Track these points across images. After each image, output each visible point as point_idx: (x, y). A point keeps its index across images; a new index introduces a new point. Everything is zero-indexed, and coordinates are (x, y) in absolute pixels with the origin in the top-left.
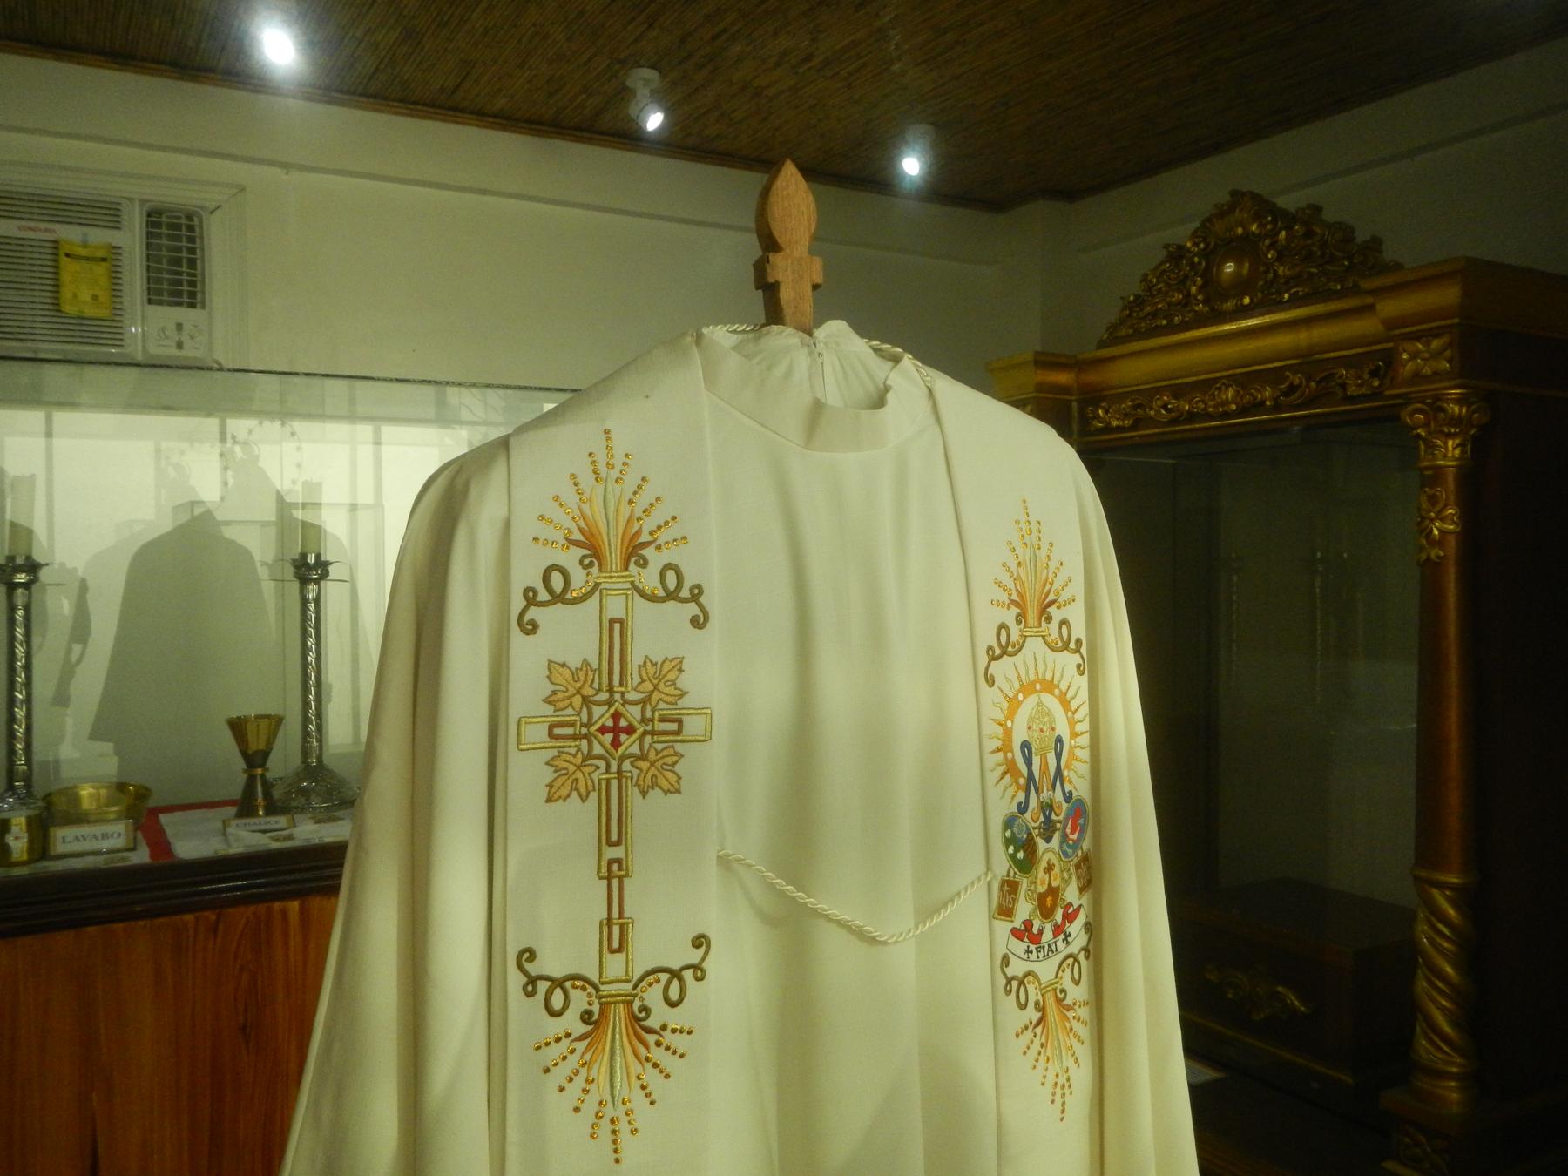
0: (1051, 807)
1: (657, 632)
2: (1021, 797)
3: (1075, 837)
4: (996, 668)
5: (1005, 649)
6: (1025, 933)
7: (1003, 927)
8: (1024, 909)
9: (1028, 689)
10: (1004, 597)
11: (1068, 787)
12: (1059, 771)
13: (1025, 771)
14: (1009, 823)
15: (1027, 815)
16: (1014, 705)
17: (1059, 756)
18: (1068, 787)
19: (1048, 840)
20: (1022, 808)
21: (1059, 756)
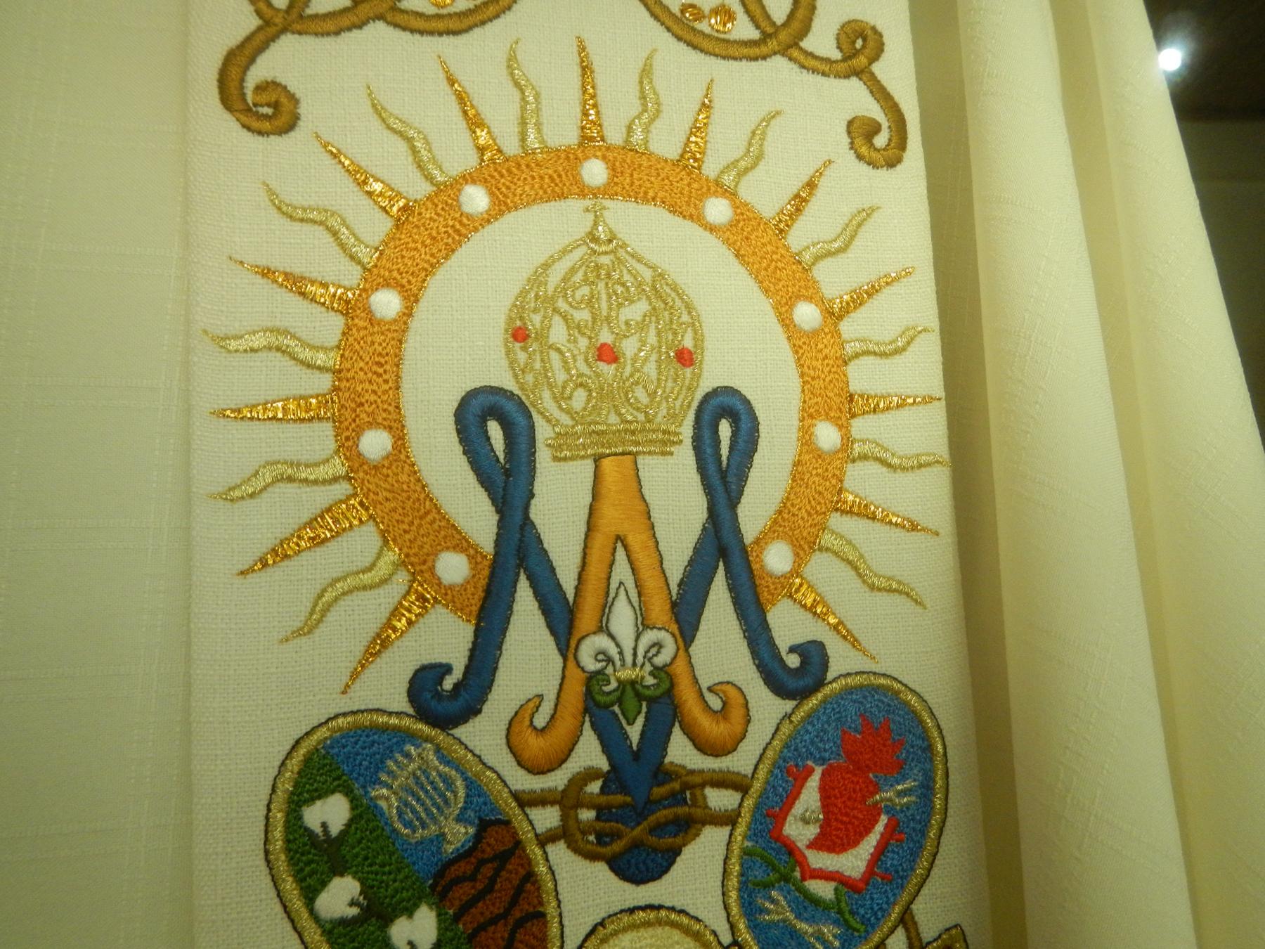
0: (663, 703)
2: (447, 639)
3: (853, 862)
9: (522, 177)
11: (788, 626)
12: (721, 545)
13: (477, 517)
15: (483, 735)
16: (424, 235)
17: (723, 482)
18: (788, 626)
19: (642, 862)
20: (444, 700)
21: (723, 482)
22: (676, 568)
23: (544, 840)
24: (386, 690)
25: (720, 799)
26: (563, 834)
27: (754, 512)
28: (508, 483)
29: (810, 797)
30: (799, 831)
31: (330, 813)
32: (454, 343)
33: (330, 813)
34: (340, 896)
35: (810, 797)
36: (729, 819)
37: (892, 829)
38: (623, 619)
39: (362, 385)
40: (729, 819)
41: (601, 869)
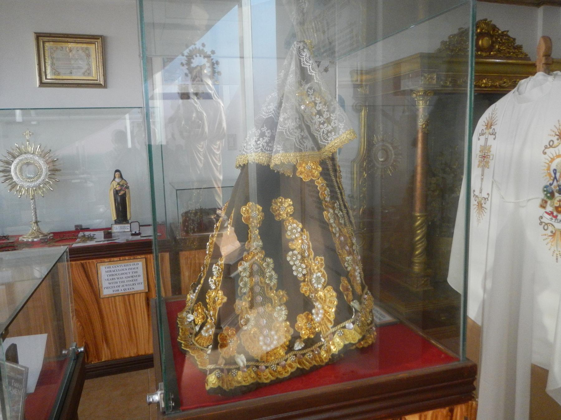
1: (491, 141)
2: (551, 182)
4: (546, 150)
5: (551, 145)
6: (551, 213)
7: (542, 211)
8: (549, 209)
10: (554, 134)
13: (553, 175)
14: (546, 187)
15: (552, 187)
16: (553, 160)
20: (551, 185)
24: (548, 184)
28: (555, 174)
31: (545, 189)
32: (554, 166)
33: (545, 189)
34: (545, 193)
39: (549, 169)
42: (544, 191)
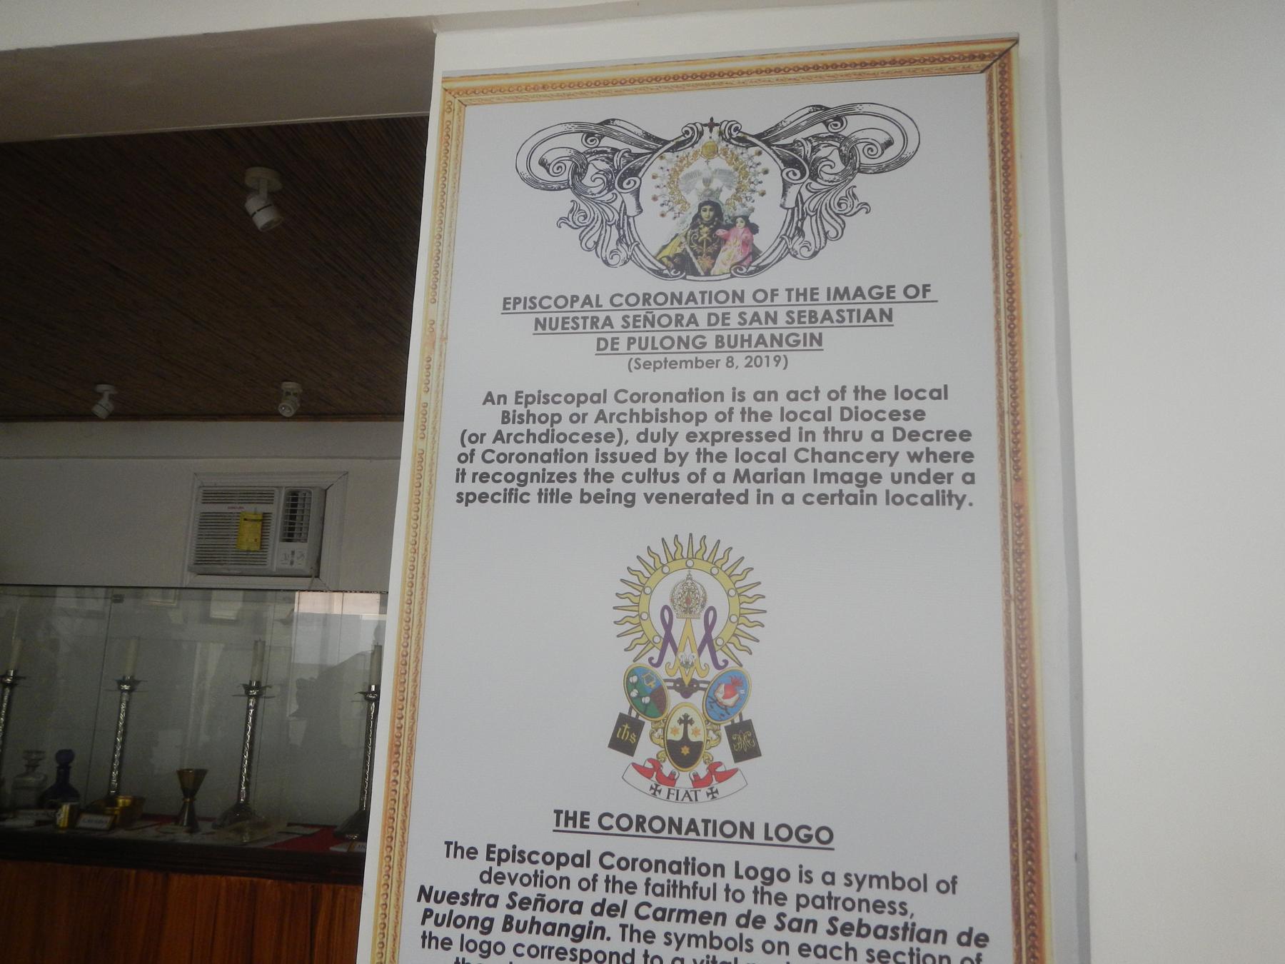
11: (721, 656)
13: (662, 632)
17: (709, 628)
21: (709, 628)
22: (699, 644)
23: (669, 688)
25: (705, 686)
26: (674, 688)
27: (714, 634)
29: (722, 688)
30: (720, 696)
34: (634, 694)
35: (722, 688)
36: (704, 689)
37: (739, 699)
38: (688, 650)
40: (704, 689)
41: (679, 694)
42: (629, 686)
